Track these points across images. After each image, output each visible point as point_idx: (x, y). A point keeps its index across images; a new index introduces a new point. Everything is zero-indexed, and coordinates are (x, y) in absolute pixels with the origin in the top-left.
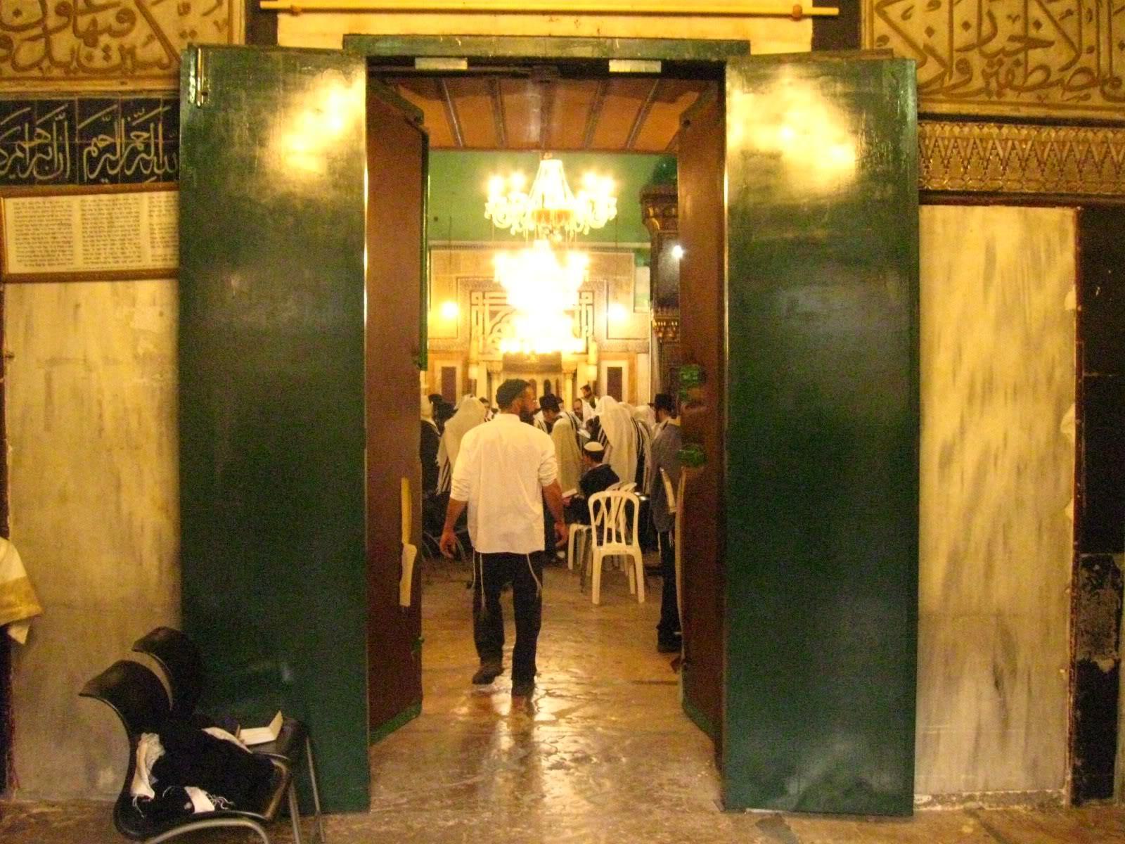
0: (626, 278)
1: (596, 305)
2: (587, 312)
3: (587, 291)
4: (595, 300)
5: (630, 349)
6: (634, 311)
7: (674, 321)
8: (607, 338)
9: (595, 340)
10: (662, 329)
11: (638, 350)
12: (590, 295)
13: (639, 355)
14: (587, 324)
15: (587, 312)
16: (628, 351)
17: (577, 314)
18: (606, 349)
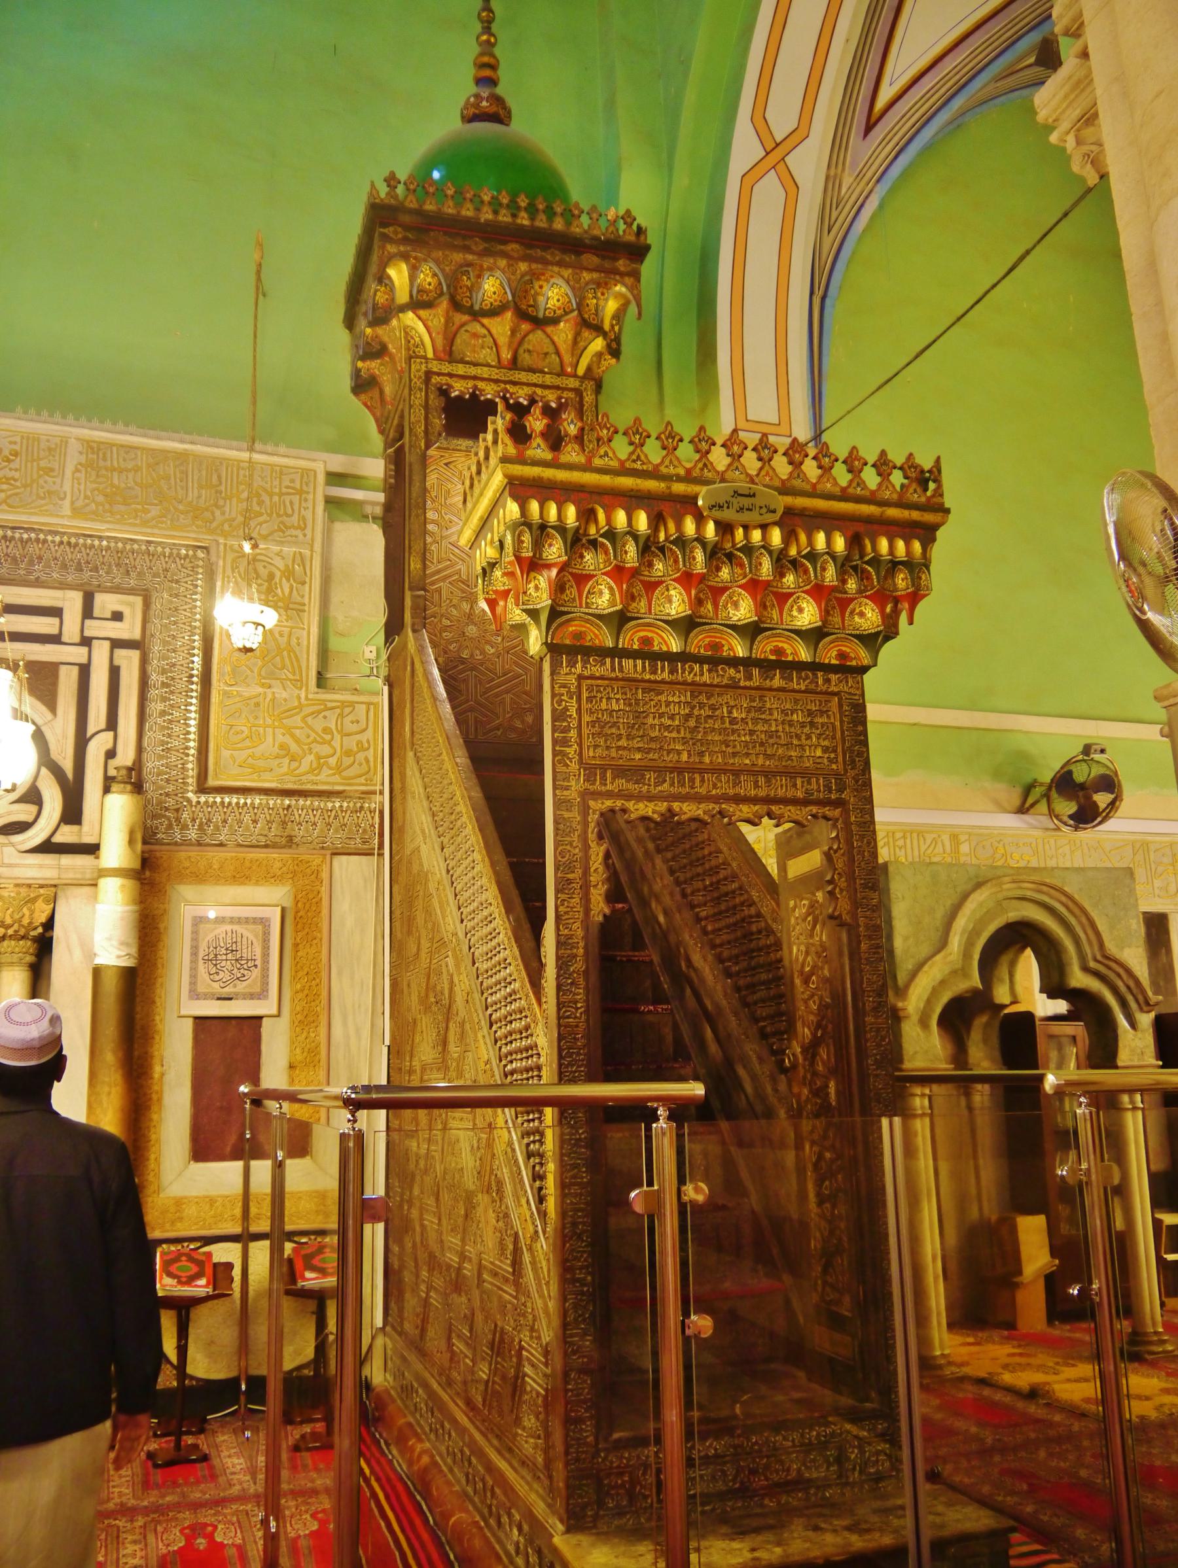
0: (288, 550)
1: (156, 648)
2: (114, 673)
3: (116, 590)
4: (155, 625)
5: (299, 833)
6: (319, 686)
7: (632, 500)
8: (202, 789)
9: (135, 780)
10: (555, 551)
11: (335, 837)
12: (131, 606)
13: (341, 862)
14: (112, 724)
15: (114, 673)
16: (290, 841)
17: (68, 681)
18: (193, 834)
